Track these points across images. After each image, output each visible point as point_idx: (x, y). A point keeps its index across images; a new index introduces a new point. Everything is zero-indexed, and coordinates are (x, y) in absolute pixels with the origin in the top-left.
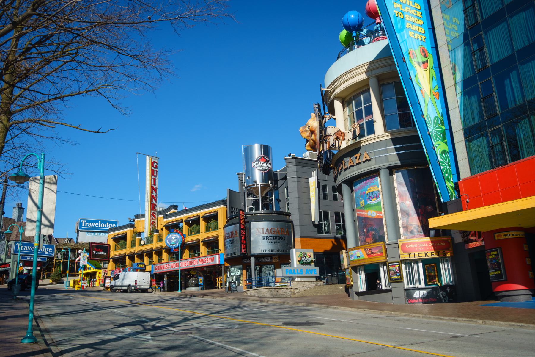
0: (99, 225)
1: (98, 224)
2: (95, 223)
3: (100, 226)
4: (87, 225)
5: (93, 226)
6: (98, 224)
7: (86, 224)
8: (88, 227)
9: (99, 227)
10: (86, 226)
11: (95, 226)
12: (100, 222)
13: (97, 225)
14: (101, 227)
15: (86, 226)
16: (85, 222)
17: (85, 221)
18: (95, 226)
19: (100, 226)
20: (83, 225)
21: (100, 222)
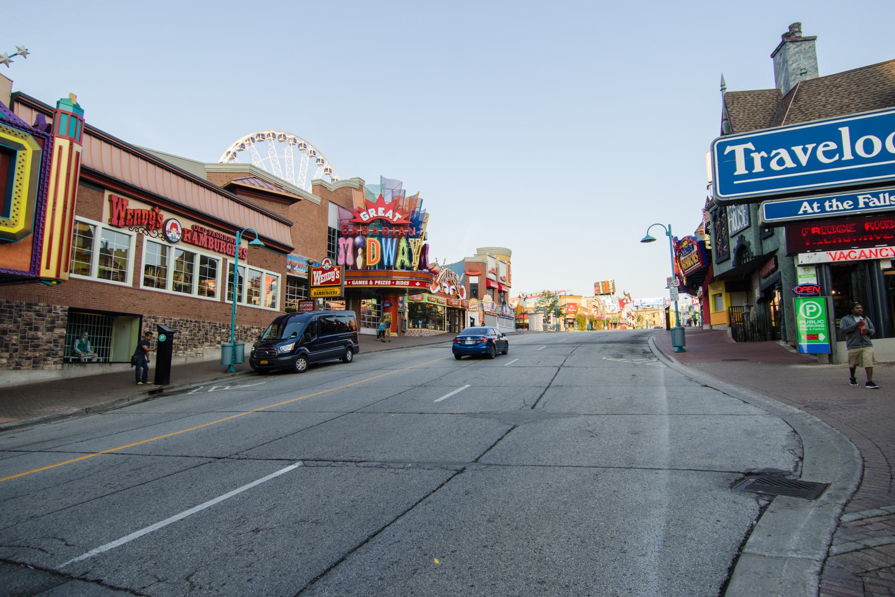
0: (840, 150)
1: (833, 146)
2: (810, 147)
3: (848, 156)
4: (765, 162)
5: (804, 160)
6: (833, 146)
7: (757, 157)
8: (768, 171)
9: (848, 163)
10: (758, 168)
11: (814, 162)
12: (845, 132)
13: (828, 154)
14: (857, 159)
15: (758, 168)
16: (747, 152)
17: (750, 146)
18: (814, 162)
19: (848, 156)
20: (741, 169)
21: (845, 132)
